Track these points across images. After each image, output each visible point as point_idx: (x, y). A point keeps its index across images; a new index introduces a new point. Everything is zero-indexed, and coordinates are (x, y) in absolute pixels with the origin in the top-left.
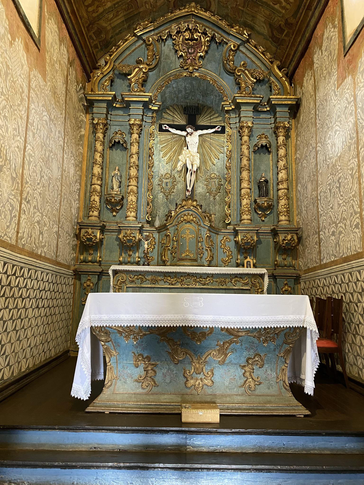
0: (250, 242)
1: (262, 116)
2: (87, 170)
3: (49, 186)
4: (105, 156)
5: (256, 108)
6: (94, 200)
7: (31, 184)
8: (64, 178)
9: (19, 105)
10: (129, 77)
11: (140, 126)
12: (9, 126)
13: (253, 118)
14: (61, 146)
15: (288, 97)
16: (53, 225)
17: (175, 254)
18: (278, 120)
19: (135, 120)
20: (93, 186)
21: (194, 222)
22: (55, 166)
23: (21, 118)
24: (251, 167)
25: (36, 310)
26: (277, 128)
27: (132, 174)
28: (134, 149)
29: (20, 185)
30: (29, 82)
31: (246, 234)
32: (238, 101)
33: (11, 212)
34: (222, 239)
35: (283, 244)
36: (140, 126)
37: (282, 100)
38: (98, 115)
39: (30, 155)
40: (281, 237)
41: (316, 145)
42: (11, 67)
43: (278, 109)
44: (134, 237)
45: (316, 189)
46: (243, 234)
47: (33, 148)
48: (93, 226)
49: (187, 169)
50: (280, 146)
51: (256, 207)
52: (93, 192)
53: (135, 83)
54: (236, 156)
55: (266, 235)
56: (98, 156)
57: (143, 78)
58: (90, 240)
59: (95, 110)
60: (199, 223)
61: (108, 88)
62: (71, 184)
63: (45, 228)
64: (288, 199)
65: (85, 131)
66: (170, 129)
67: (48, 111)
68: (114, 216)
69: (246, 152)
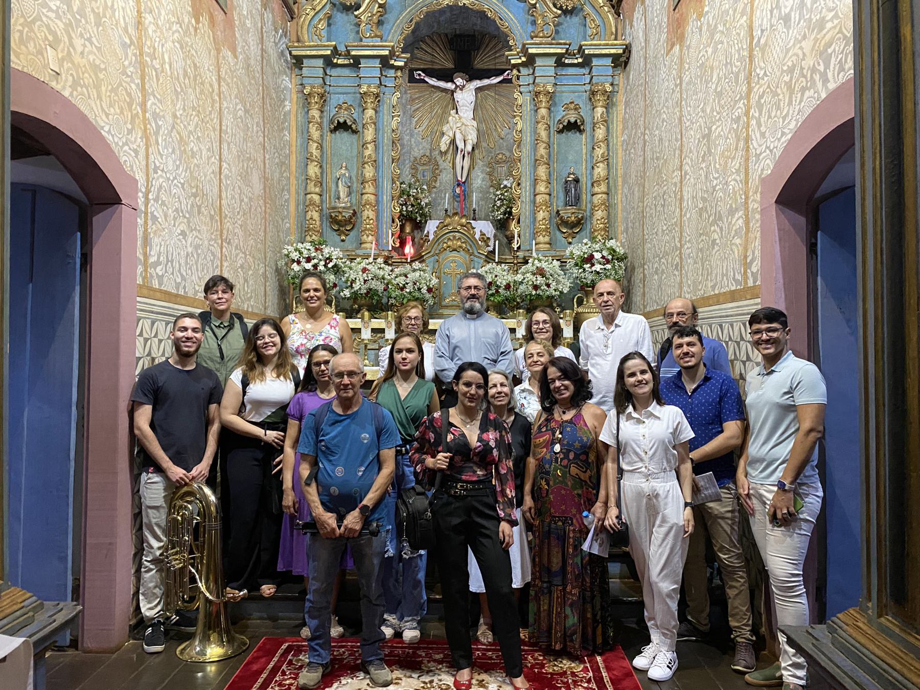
1: (571, 71)
3: (250, 209)
4: (324, 146)
5: (560, 62)
8: (268, 191)
9: (210, 113)
10: (356, 13)
14: (260, 144)
18: (594, 81)
19: (369, 86)
20: (309, 196)
22: (255, 178)
23: (214, 130)
26: (593, 93)
27: (367, 175)
28: (369, 134)
30: (219, 71)
32: (530, 51)
33: (213, 262)
38: (311, 81)
39: (227, 177)
43: (595, 62)
49: (457, 148)
52: (310, 205)
59: (305, 71)
61: (324, 33)
62: (276, 196)
63: (250, 272)
65: (291, 105)
66: (427, 79)
67: (243, 102)
68: (343, 241)
69: (543, 134)
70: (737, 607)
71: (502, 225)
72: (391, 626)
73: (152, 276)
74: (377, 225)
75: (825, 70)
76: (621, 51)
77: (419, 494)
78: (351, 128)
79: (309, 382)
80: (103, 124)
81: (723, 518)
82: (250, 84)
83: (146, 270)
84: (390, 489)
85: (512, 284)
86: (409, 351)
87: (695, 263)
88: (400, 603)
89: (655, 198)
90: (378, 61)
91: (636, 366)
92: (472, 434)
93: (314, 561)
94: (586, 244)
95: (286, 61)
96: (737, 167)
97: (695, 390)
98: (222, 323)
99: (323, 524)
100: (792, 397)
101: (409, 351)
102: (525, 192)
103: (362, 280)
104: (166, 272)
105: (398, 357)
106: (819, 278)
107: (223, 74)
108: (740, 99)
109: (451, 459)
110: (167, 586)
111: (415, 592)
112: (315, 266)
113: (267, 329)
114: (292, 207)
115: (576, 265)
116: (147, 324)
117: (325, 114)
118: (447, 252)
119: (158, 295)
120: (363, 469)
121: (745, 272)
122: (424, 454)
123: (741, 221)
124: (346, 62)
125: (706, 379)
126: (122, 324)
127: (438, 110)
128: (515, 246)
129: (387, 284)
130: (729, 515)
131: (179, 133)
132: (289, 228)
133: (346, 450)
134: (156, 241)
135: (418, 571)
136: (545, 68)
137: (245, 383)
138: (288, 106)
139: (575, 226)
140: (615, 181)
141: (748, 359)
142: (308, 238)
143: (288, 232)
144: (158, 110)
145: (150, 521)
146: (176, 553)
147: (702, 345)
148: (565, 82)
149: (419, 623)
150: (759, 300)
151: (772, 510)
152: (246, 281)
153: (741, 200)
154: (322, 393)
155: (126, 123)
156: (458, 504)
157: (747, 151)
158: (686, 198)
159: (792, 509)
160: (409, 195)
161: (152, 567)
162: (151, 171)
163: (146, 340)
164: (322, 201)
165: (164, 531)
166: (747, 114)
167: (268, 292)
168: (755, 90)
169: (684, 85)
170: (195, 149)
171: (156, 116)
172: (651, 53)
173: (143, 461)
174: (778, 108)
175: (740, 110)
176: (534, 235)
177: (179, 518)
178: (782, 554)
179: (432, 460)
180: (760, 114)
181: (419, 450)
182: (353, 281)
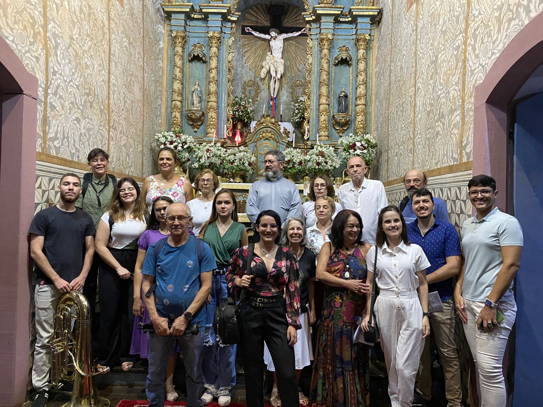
4: (185, 70)
6: (175, 117)
7: (116, 112)
8: (146, 97)
9: (102, 41)
11: (219, 39)
12: (95, 63)
14: (141, 66)
15: (369, 7)
16: (138, 145)
18: (358, 33)
19: (214, 32)
20: (174, 102)
22: (136, 88)
23: (104, 52)
24: (330, 81)
26: (358, 40)
27: (212, 89)
28: (213, 63)
29: (107, 116)
30: (109, 14)
32: (318, 12)
33: (102, 141)
38: (176, 28)
39: (114, 85)
42: (92, 6)
43: (359, 20)
47: (116, 77)
49: (271, 76)
52: (174, 108)
62: (152, 101)
63: (131, 150)
65: (164, 44)
66: (253, 32)
67: (128, 37)
68: (196, 132)
69: (325, 66)
70: (451, 386)
71: (299, 126)
72: (211, 393)
73: (50, 148)
74: (218, 123)
75: (528, 4)
76: (376, 13)
77: (229, 304)
78: (202, 60)
79: (154, 222)
80: (7, 35)
81: (444, 323)
82: (134, 26)
83: (45, 142)
84: (210, 298)
85: (303, 162)
86: (227, 202)
87: (424, 148)
88: (217, 377)
89: (397, 106)
90: (220, 16)
91: (391, 216)
92: (269, 261)
93: (151, 351)
94: (351, 137)
95: (161, 15)
96: (457, 79)
97: (427, 234)
98: (100, 181)
99: (158, 325)
100: (498, 240)
101: (227, 202)
102: (313, 104)
103: (206, 157)
104: (62, 144)
105: (219, 207)
106: (515, 156)
107: (112, 16)
108: (460, 34)
109: (252, 279)
110: (54, 364)
111: (228, 370)
112: (176, 147)
113: (127, 185)
114: (163, 110)
115: (345, 150)
116: (45, 180)
117: (186, 50)
118: (262, 140)
119: (56, 160)
120: (188, 286)
121: (461, 152)
122: (235, 274)
123: (458, 118)
124: (200, 17)
125: (435, 226)
126: (22, 178)
127: (259, 52)
128: (306, 138)
129: (223, 160)
130: (449, 321)
131: (75, 51)
132: (161, 123)
133: (175, 273)
134: (54, 123)
135: (231, 356)
136: (327, 24)
137: (111, 223)
138: (162, 44)
139: (344, 126)
140: (371, 97)
141: (462, 212)
142: (173, 129)
143: (160, 125)
144: (57, 32)
145: (40, 319)
146: (59, 341)
147: (433, 202)
148: (340, 33)
149: (230, 391)
150: (471, 172)
151: (480, 320)
152: (128, 155)
153: (459, 103)
154: (162, 230)
155: (28, 37)
156: (257, 313)
157: (465, 68)
158: (418, 105)
159: (495, 321)
160: (240, 105)
161: (41, 351)
162: (50, 74)
163: (44, 192)
164: (182, 106)
165: (51, 326)
166: (465, 43)
167: (145, 163)
168: (471, 25)
169: (419, 29)
170: (88, 63)
171: (55, 36)
172: (396, 12)
173: (37, 275)
174: (490, 36)
175: (459, 41)
176: (318, 131)
177: (62, 317)
178: (487, 353)
179: (239, 279)
180: (475, 42)
181: (233, 272)
182: (200, 158)
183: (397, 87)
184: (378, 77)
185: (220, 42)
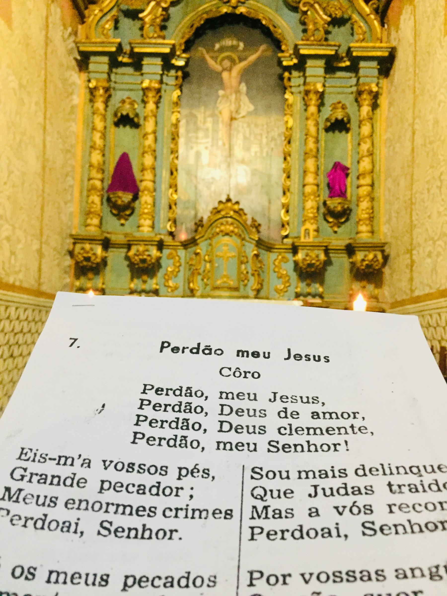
0: (314, 264)
2: (83, 157)
3: (23, 184)
8: (47, 170)
10: (141, 15)
11: (158, 91)
13: (325, 77)
17: (208, 280)
18: (362, 81)
19: (151, 81)
20: (92, 182)
21: (236, 234)
25: (10, 360)
26: (360, 93)
28: (149, 126)
31: (309, 252)
34: (276, 257)
35: (362, 265)
36: (158, 91)
37: (369, 49)
40: (359, 256)
41: (414, 121)
43: (362, 64)
44: (149, 255)
45: (410, 187)
46: (305, 251)
48: (91, 240)
50: (364, 120)
51: (326, 212)
53: (151, 25)
54: (298, 136)
55: (339, 253)
56: (97, 137)
57: (162, 17)
58: (87, 259)
59: (92, 67)
60: (243, 236)
61: (111, 33)
64: (372, 199)
68: (122, 225)
69: (313, 130)
74: (154, 211)
89: (428, 182)
90: (159, 59)
118: (220, 235)
140: (379, 176)
183: (428, 153)
184: (390, 146)
185: (160, 97)
